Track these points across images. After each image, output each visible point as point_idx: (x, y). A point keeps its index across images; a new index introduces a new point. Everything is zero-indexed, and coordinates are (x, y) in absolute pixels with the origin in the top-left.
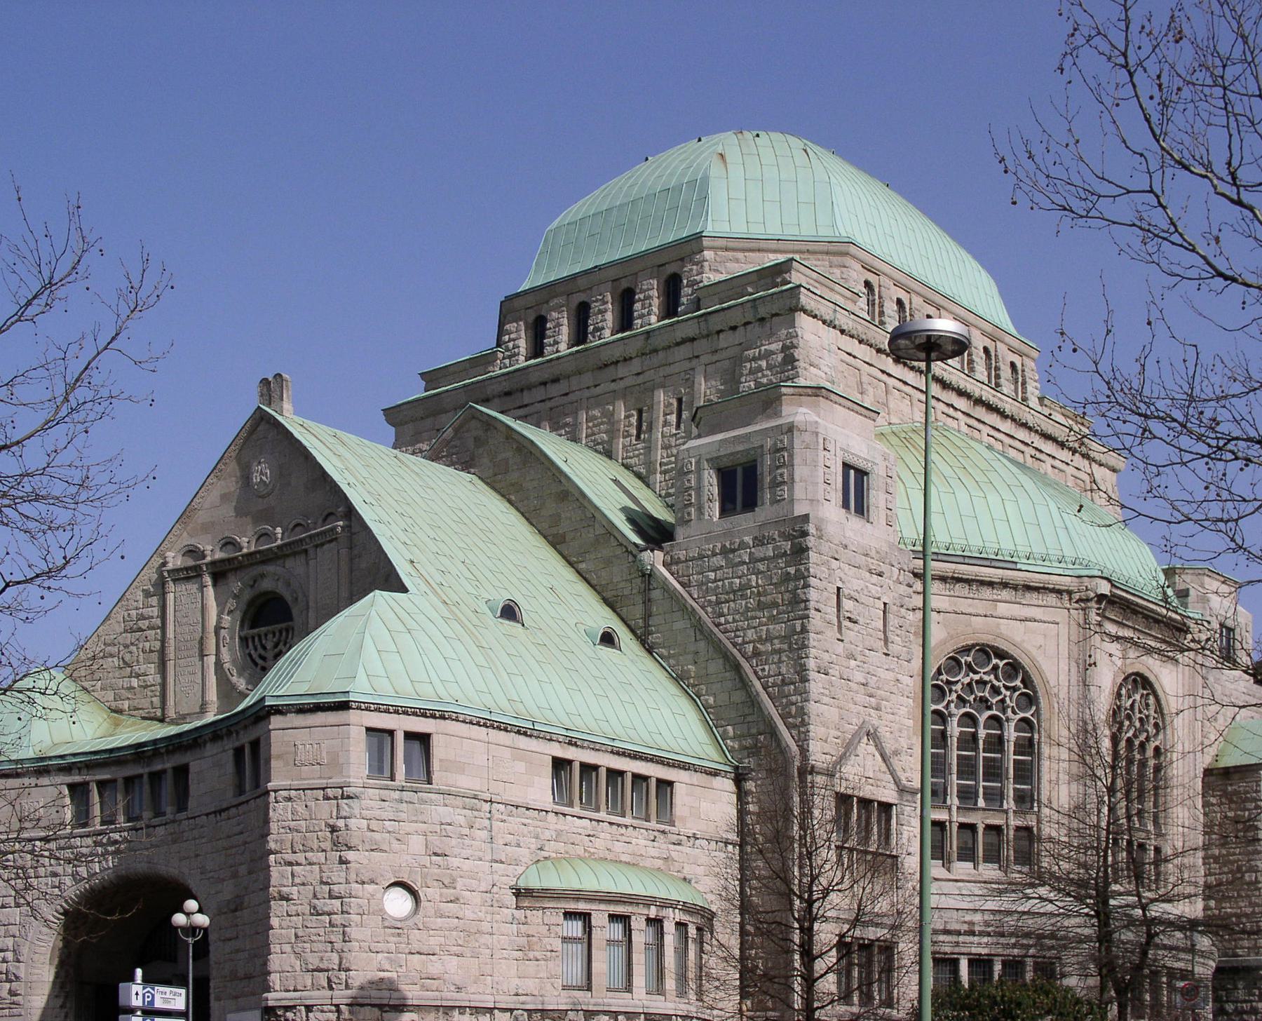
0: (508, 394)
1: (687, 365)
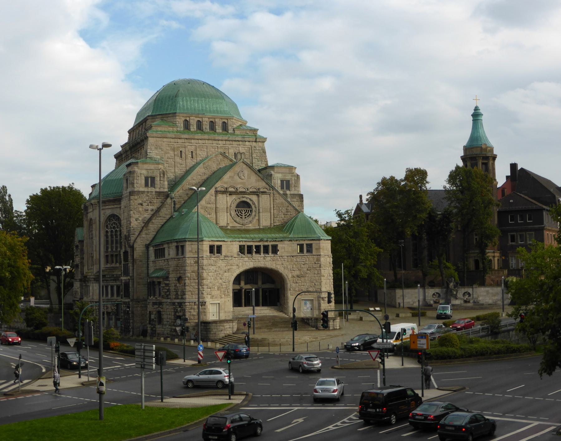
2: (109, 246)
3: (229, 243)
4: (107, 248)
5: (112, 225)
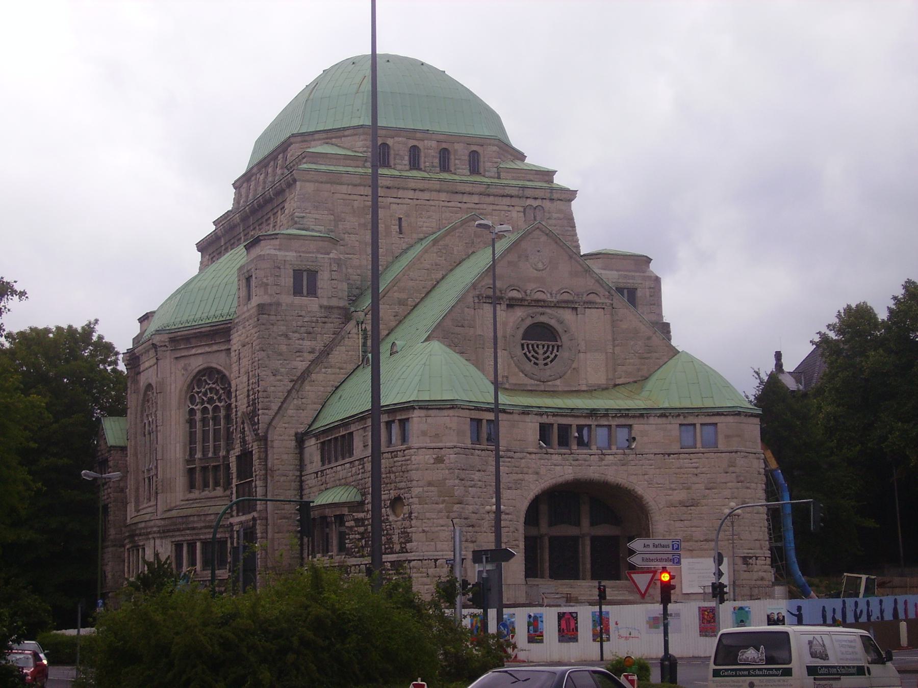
0: (388, 188)
1: (506, 208)
2: (199, 447)
3: (516, 417)
4: (192, 451)
5: (205, 394)
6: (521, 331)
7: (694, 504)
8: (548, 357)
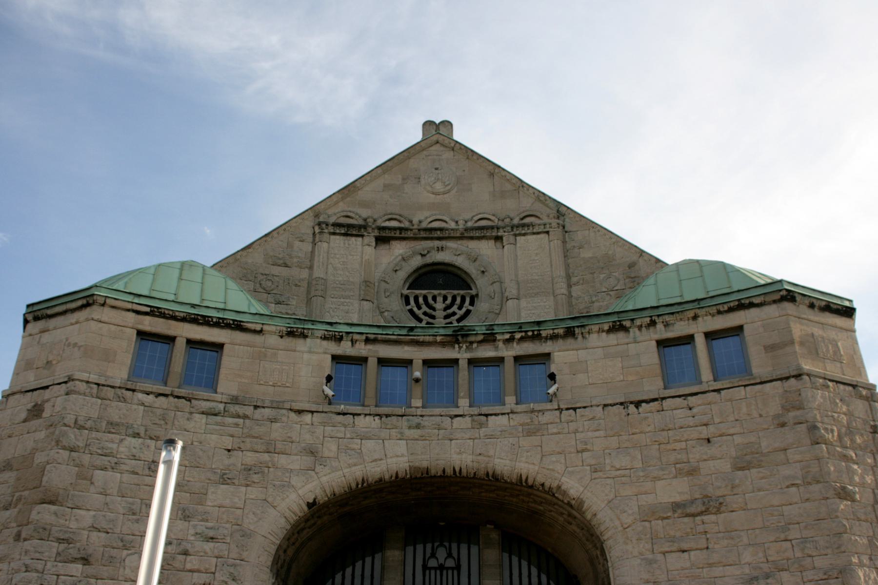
6: (402, 275)
7: (711, 505)
8: (454, 314)
